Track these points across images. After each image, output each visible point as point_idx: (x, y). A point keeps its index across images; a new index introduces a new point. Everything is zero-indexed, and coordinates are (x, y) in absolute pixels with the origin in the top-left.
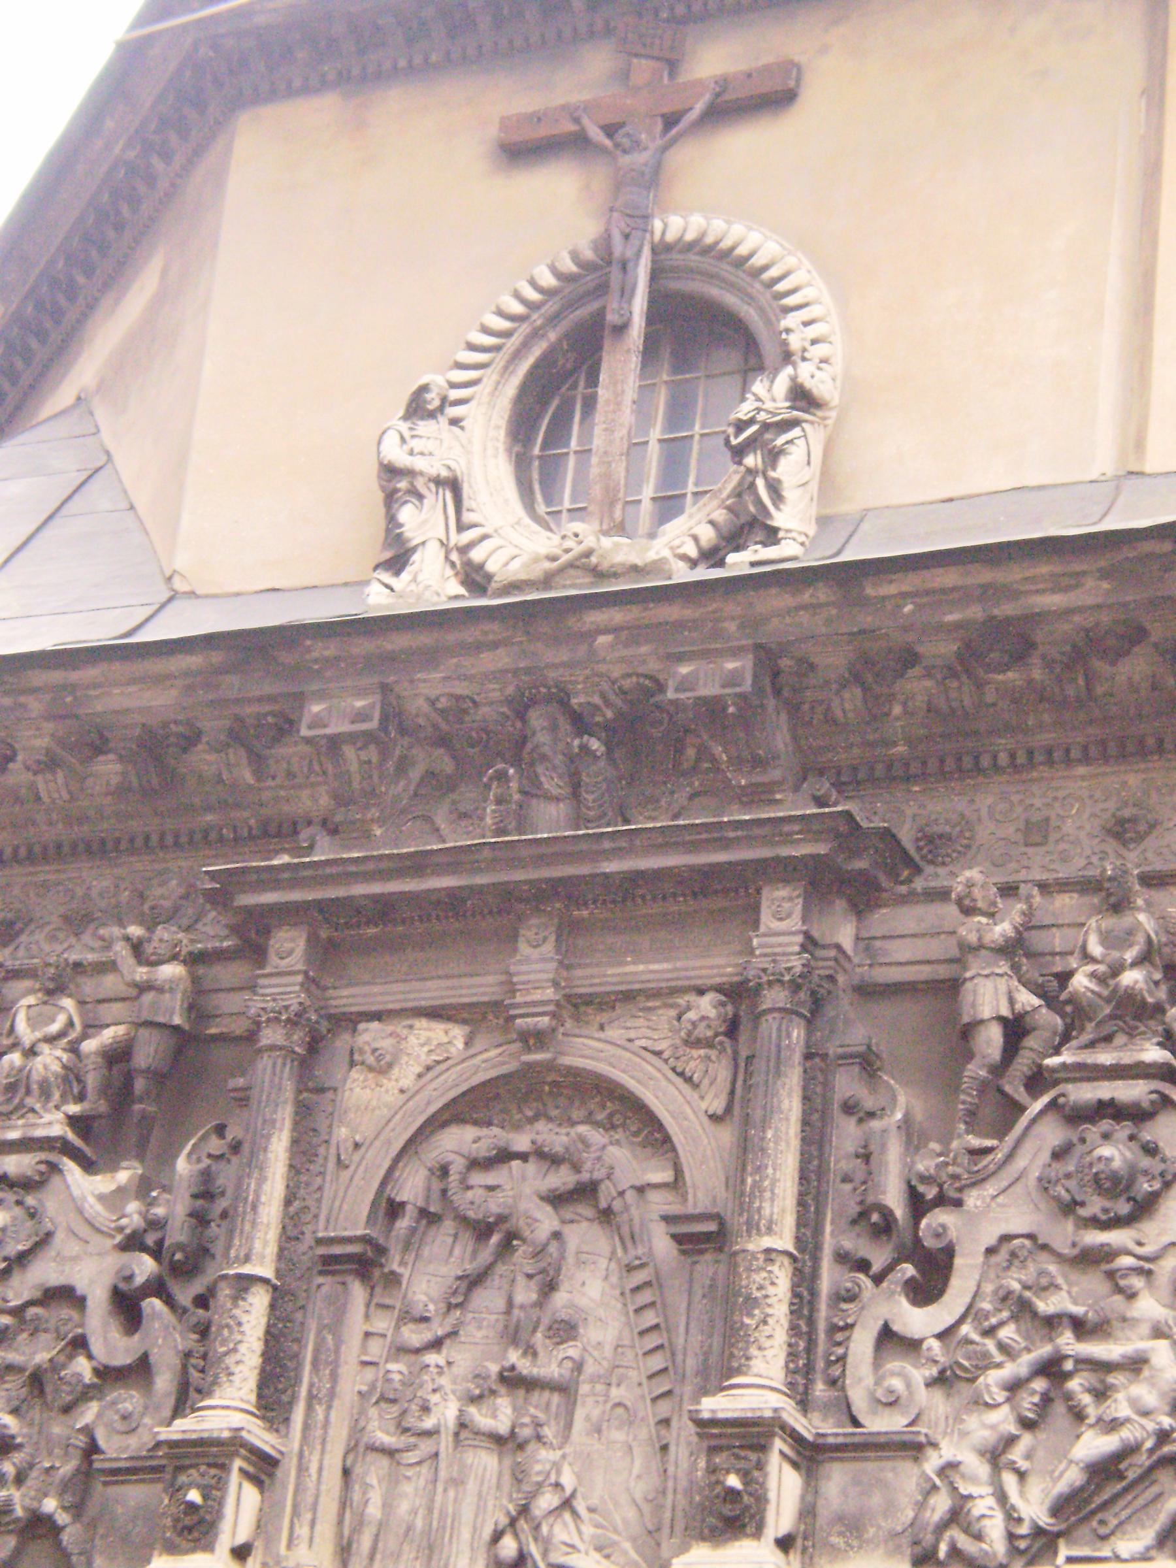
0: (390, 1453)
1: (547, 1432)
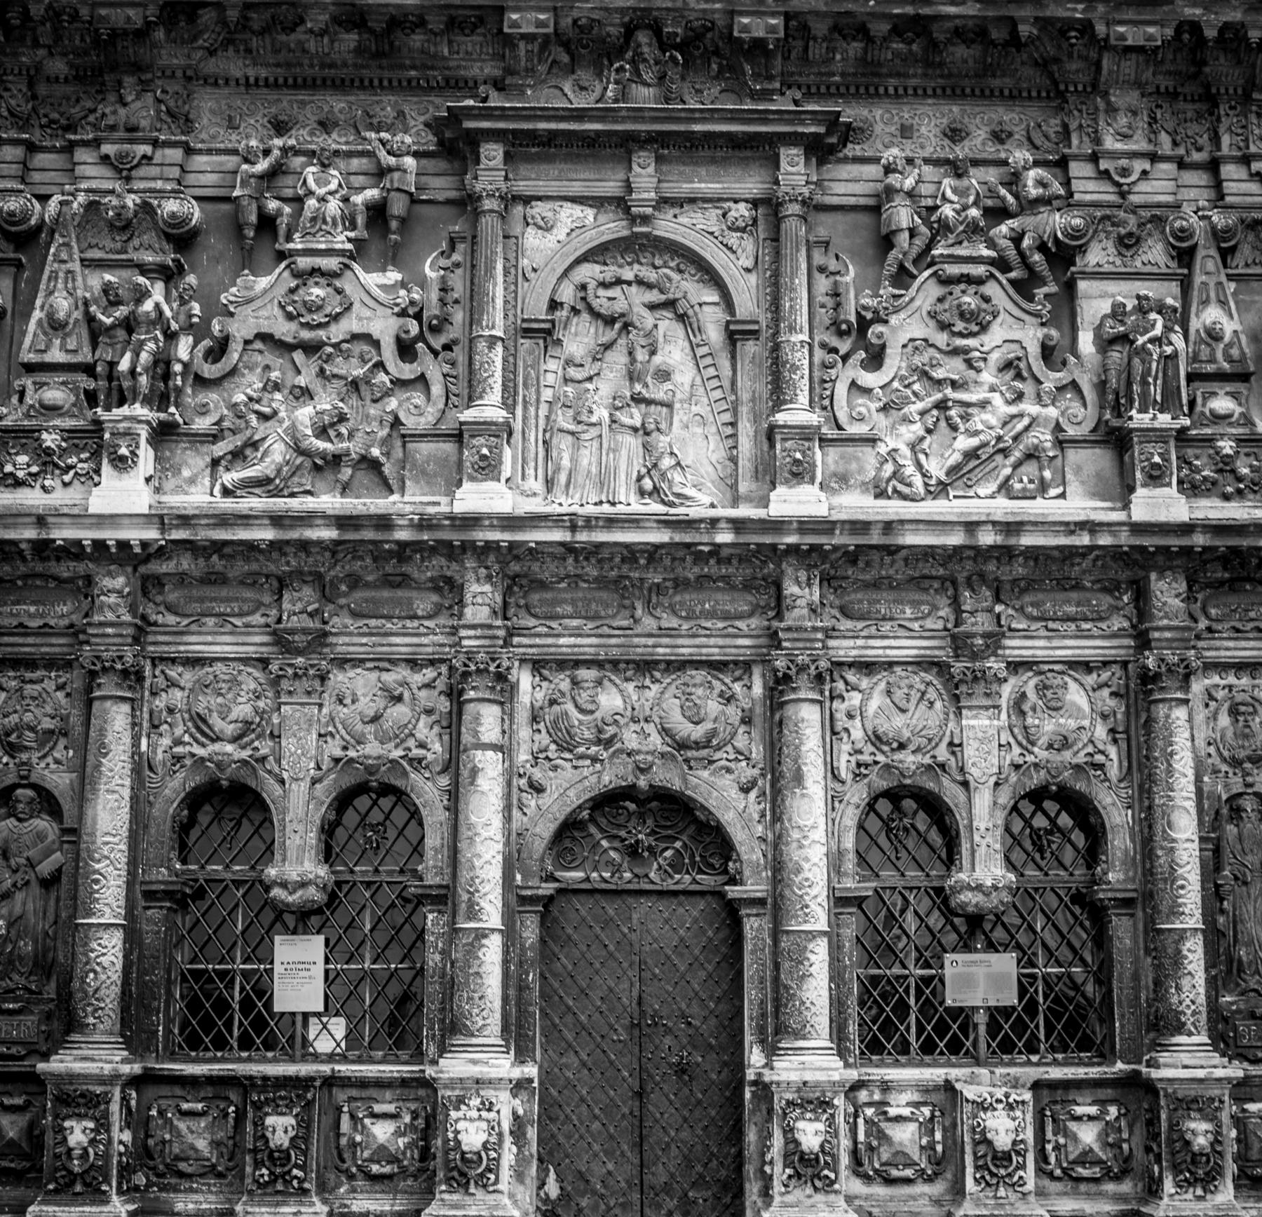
0: (572, 433)
1: (663, 426)
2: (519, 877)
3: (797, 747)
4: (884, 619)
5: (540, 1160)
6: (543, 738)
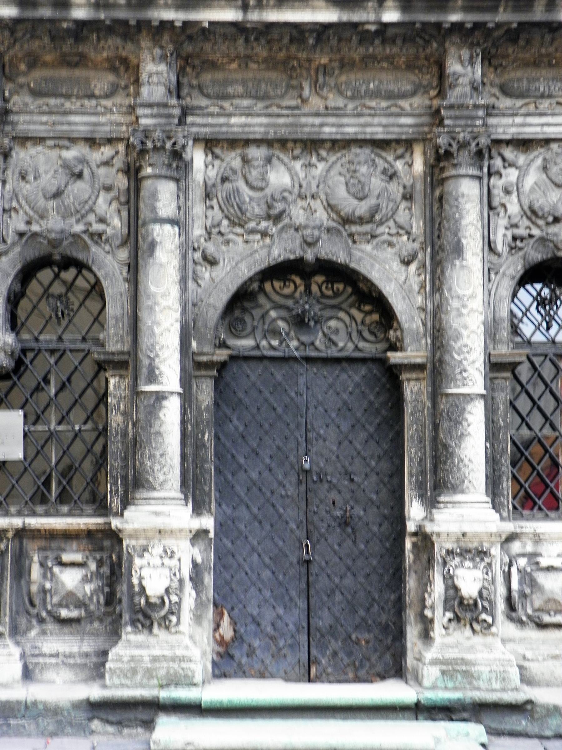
3: (457, 221)
4: (542, 96)
5: (215, 605)
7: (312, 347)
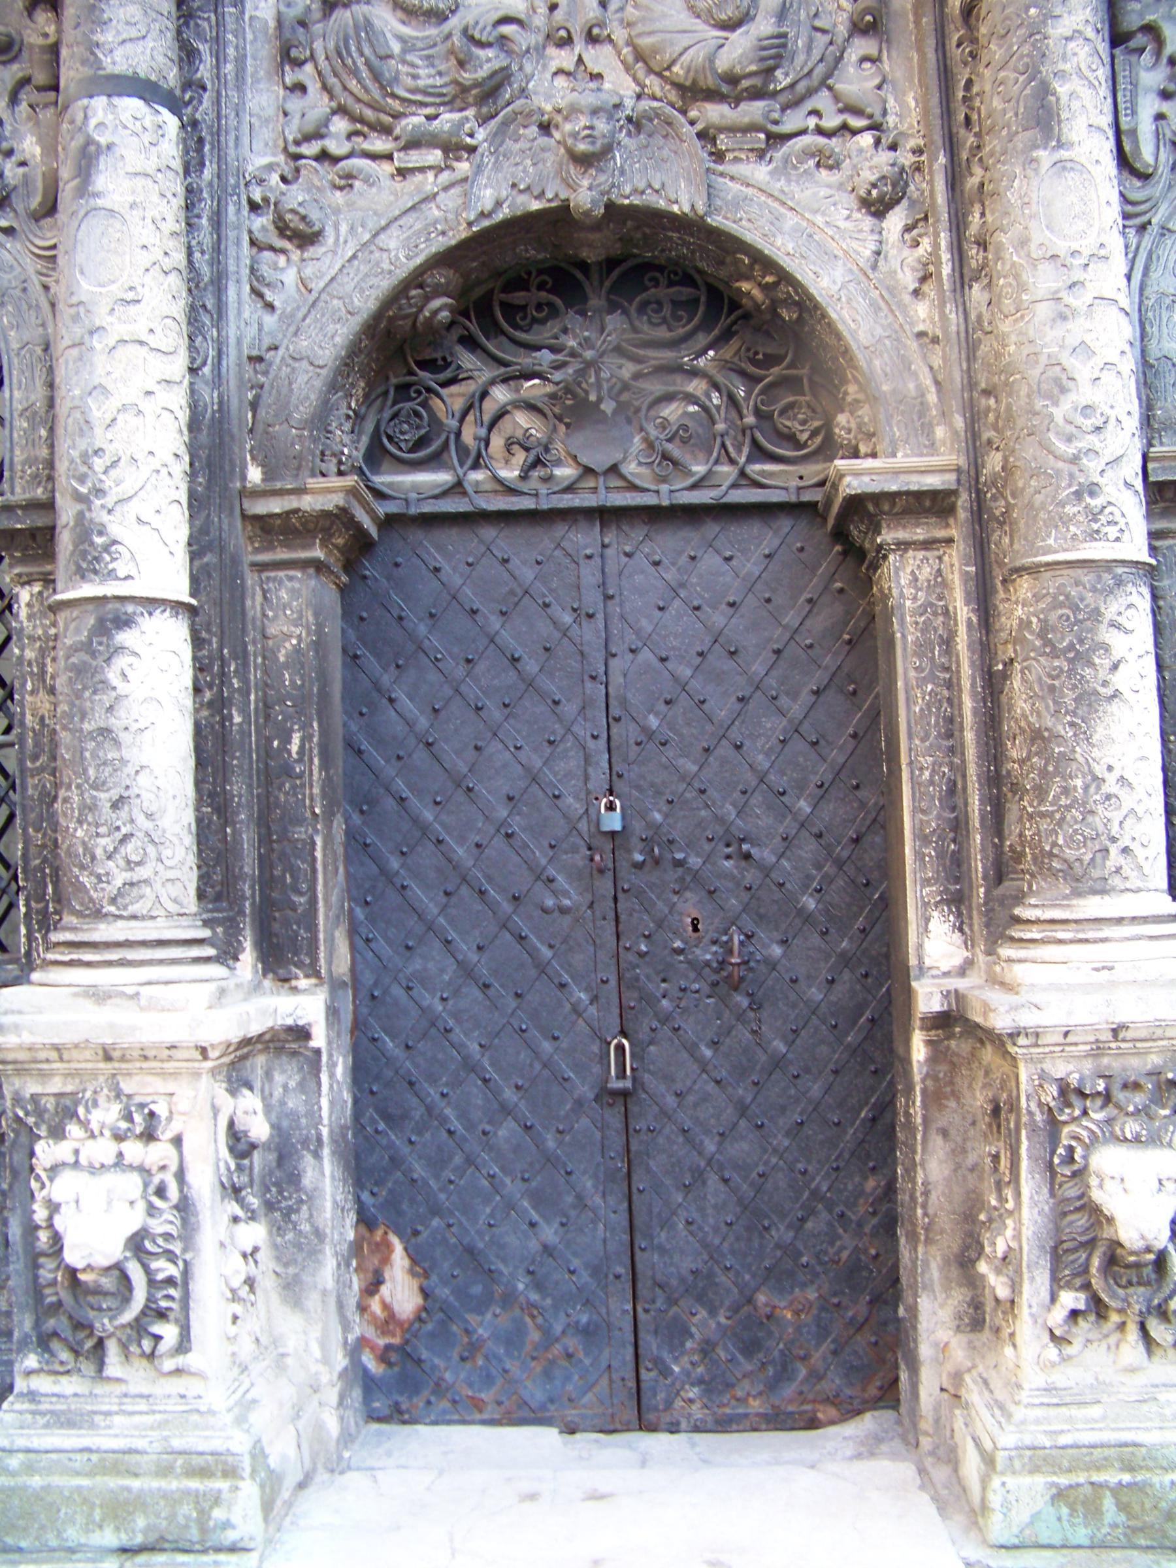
2: (255, 475)
6: (316, 104)
7: (615, 482)
